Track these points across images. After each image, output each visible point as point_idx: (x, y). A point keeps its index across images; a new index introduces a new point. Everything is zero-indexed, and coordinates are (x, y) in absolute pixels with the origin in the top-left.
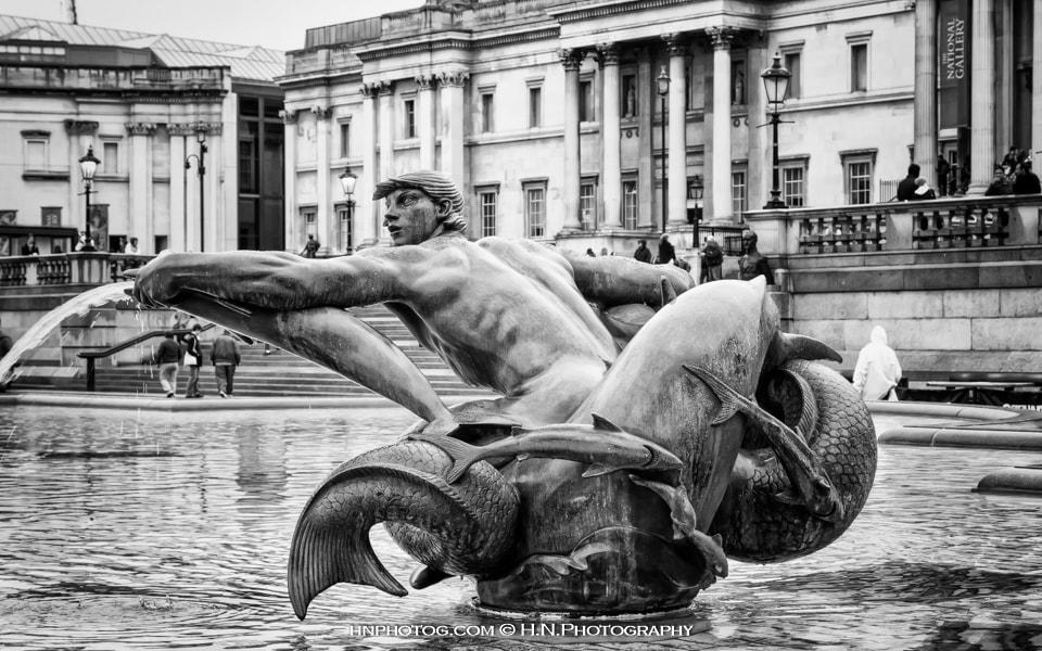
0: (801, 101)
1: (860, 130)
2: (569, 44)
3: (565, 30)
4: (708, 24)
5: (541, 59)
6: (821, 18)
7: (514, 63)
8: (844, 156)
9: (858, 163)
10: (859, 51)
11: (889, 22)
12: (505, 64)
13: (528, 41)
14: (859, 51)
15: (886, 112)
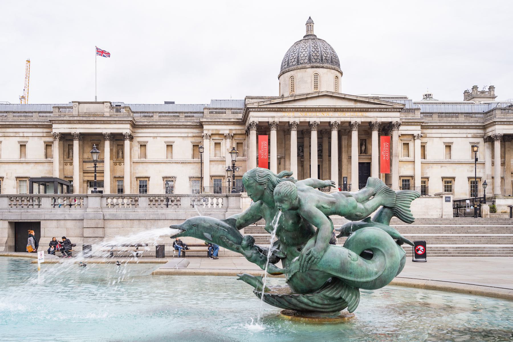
0: (147, 160)
1: (169, 170)
2: (57, 131)
3: (54, 126)
4: (124, 132)
5: (25, 135)
6: (155, 135)
7: (12, 135)
8: (164, 178)
9: (169, 181)
10: (169, 146)
11: (181, 139)
12: (6, 134)
13: (21, 128)
14: (169, 146)
15: (179, 165)
